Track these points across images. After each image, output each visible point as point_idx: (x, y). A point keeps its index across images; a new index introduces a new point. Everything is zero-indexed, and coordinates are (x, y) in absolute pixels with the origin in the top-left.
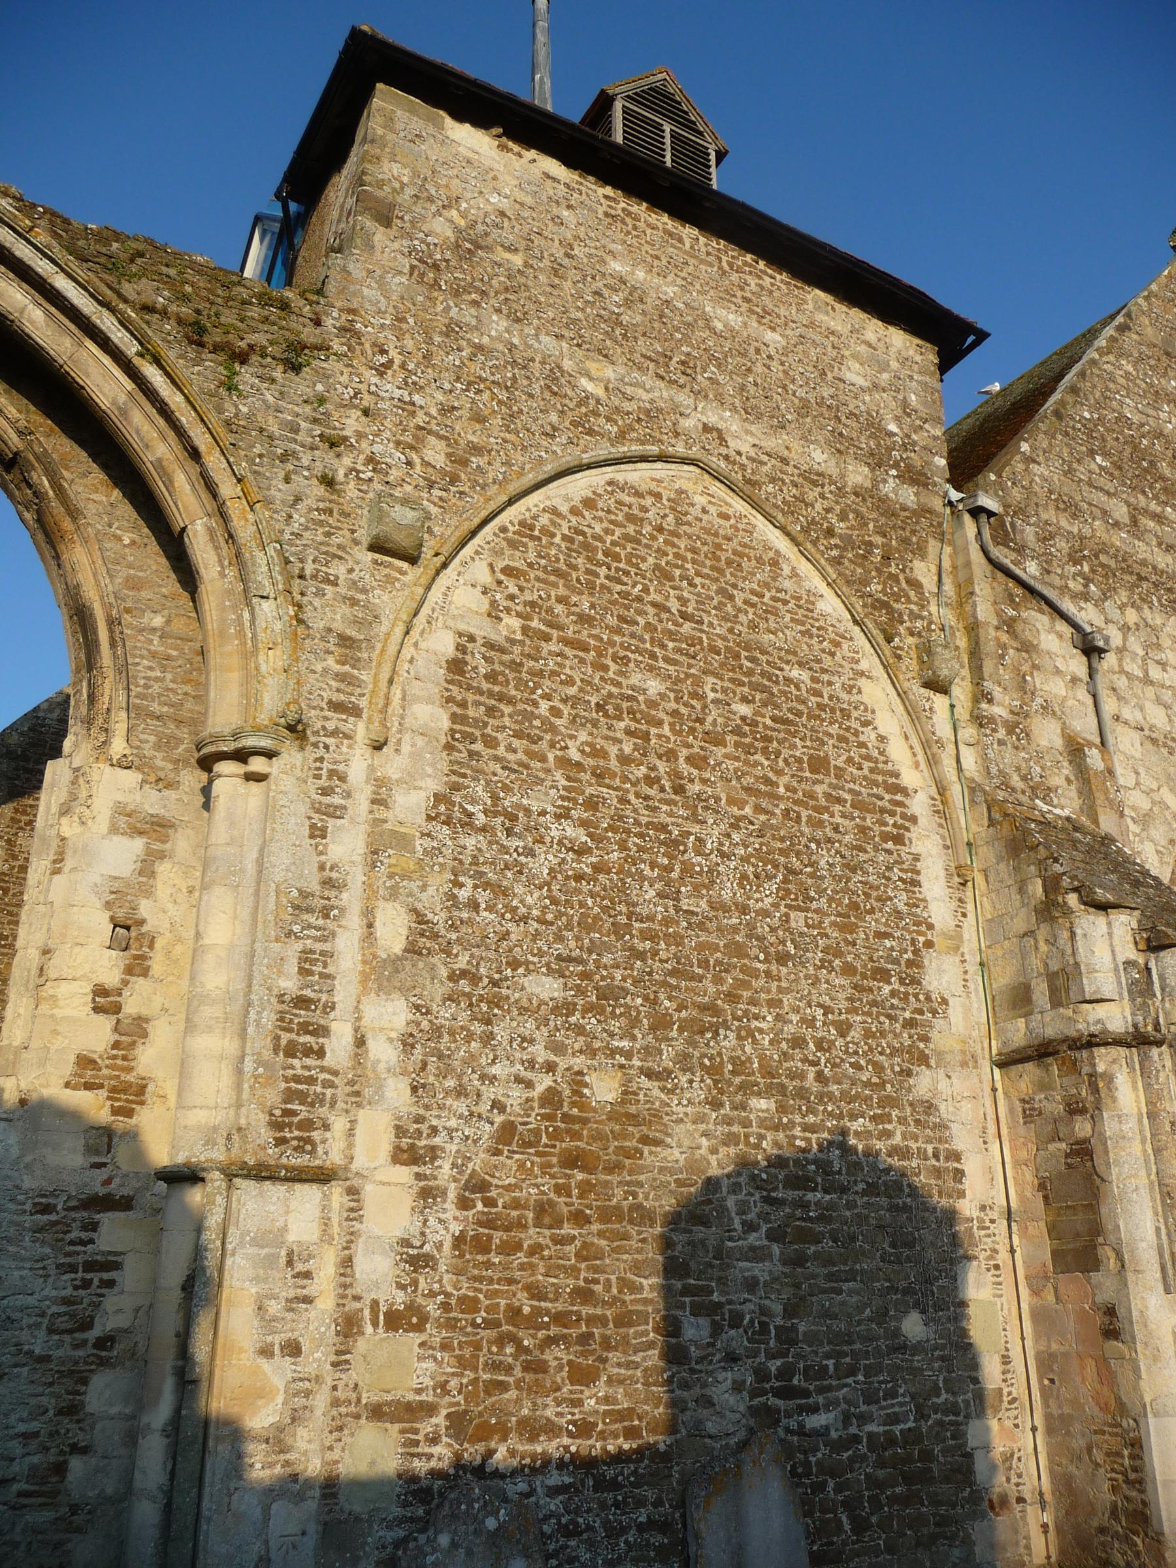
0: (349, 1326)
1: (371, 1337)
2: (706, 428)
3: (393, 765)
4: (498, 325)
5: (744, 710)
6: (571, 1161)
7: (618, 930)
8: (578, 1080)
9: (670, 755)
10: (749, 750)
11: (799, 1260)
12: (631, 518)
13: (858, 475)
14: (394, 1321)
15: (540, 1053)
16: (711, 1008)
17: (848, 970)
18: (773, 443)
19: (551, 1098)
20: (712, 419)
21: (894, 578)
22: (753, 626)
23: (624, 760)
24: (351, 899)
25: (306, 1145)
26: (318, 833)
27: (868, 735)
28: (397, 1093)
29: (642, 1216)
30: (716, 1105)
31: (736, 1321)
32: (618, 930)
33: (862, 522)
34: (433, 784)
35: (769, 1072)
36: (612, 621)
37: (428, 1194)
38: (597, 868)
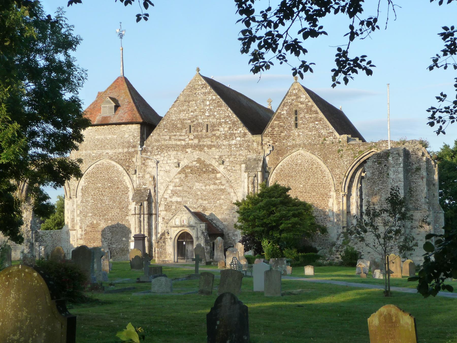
0: (77, 239)
1: (79, 240)
2: (106, 153)
3: (77, 199)
4: (84, 152)
5: (109, 184)
6: (93, 228)
7: (96, 209)
8: (93, 221)
9: (102, 191)
10: (110, 189)
11: (113, 234)
12: (98, 168)
13: (126, 150)
14: (80, 239)
15: (90, 220)
16: (105, 214)
17: (119, 208)
18: (114, 151)
19: (91, 223)
20: (107, 152)
21: (130, 162)
22: (111, 175)
23: (97, 193)
24: (75, 210)
25: (74, 228)
26: (73, 206)
27: (124, 183)
28: (79, 224)
29: (99, 231)
30: (105, 222)
31: (106, 239)
32: (96, 209)
33: (126, 156)
34: (81, 200)
35: (110, 219)
36: (96, 180)
37: (82, 231)
38: (95, 204)
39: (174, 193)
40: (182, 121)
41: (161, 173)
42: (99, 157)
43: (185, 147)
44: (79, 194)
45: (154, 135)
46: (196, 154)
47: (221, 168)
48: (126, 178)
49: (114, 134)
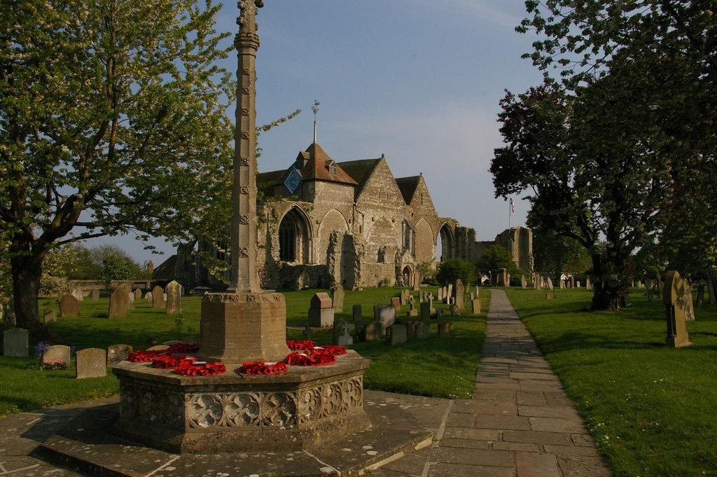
39: (372, 239)
40: (376, 188)
41: (365, 224)
42: (331, 206)
43: (378, 207)
44: (320, 235)
45: (362, 197)
46: (382, 214)
47: (393, 225)
48: (346, 225)
49: (340, 190)
